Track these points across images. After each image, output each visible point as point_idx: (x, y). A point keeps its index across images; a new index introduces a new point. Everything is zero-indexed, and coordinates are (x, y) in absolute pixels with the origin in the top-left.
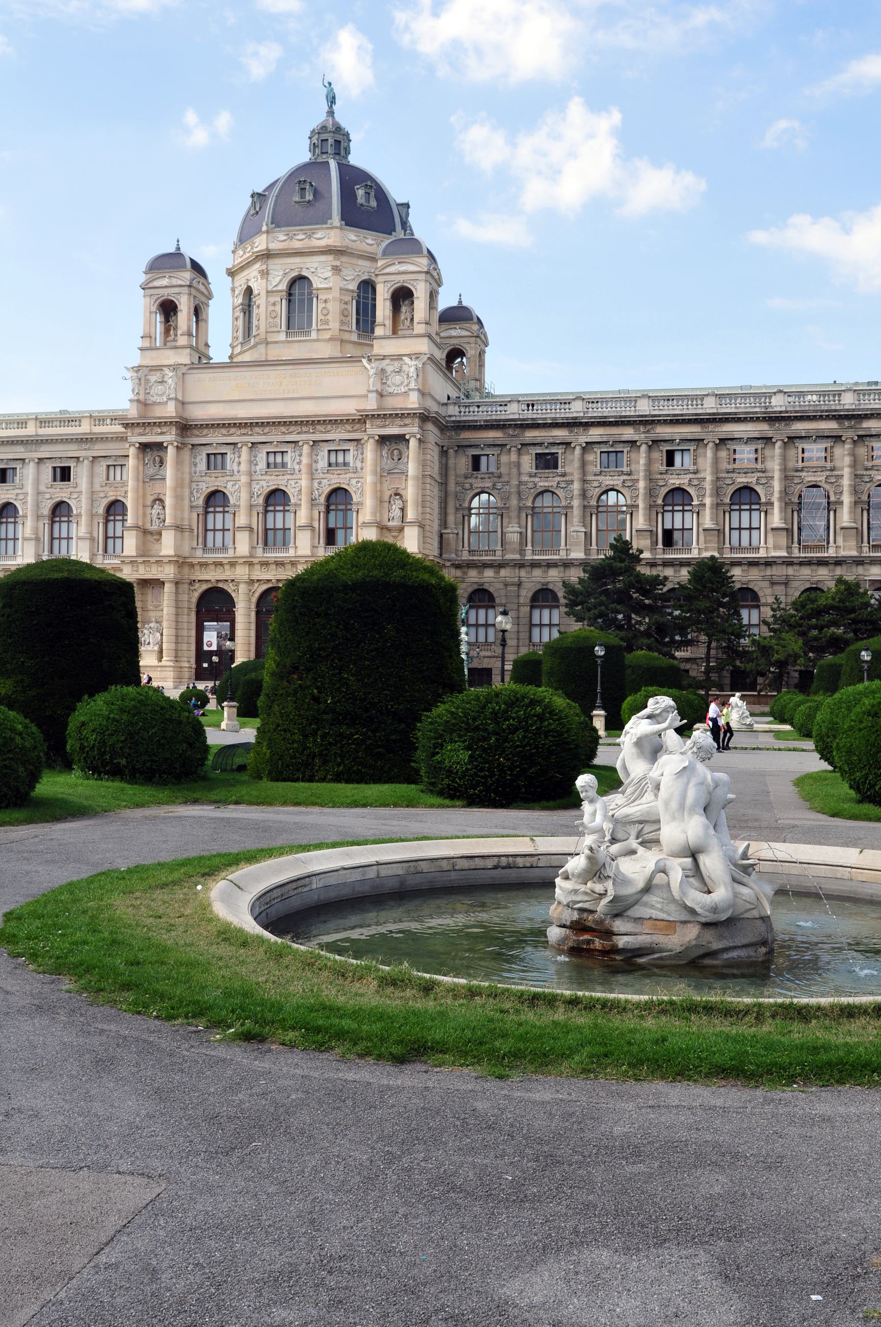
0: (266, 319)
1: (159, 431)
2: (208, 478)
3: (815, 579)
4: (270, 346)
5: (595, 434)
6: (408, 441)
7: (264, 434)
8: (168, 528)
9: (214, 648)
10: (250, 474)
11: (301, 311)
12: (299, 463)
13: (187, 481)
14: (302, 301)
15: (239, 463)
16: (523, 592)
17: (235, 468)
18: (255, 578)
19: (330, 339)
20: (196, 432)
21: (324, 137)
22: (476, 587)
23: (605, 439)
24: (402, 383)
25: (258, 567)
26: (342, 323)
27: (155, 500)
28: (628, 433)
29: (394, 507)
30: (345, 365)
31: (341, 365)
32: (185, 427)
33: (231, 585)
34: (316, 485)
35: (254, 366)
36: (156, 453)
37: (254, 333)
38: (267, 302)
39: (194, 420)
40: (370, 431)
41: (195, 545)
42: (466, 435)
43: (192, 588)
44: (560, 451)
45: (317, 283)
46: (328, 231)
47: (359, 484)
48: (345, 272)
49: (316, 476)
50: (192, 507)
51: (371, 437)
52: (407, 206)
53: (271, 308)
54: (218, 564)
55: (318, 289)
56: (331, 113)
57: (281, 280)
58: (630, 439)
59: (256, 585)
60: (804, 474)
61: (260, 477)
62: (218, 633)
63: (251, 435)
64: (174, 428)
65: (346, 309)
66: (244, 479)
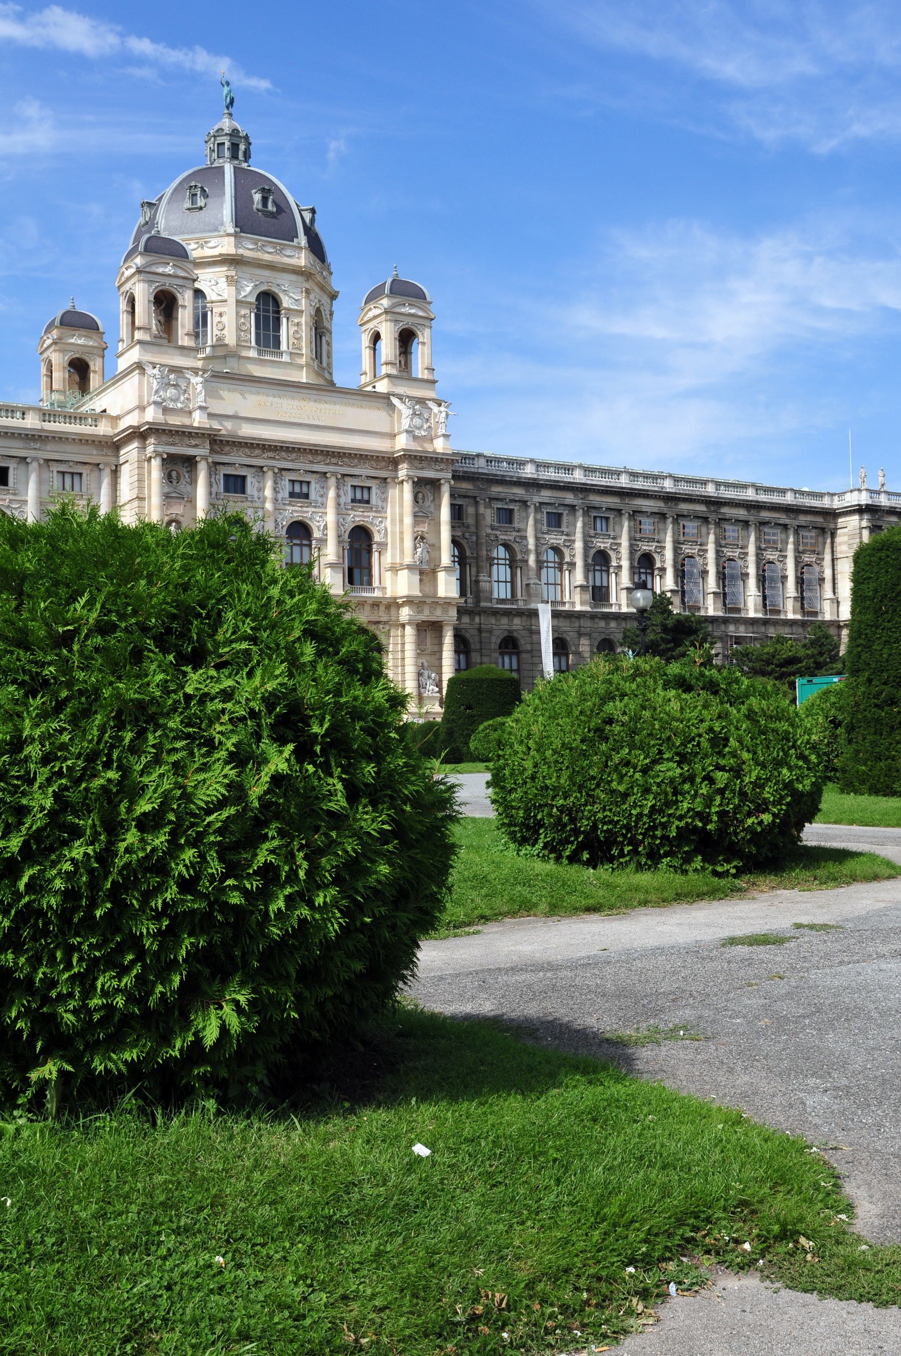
1: (194, 443)
4: (241, 361)
5: (546, 495)
7: (292, 461)
11: (266, 328)
16: (494, 640)
17: (256, 494)
21: (236, 141)
23: (552, 501)
28: (570, 498)
32: (216, 442)
35: (278, 384)
44: (516, 508)
45: (286, 302)
55: (289, 309)
58: (571, 503)
60: (684, 547)
63: (278, 460)
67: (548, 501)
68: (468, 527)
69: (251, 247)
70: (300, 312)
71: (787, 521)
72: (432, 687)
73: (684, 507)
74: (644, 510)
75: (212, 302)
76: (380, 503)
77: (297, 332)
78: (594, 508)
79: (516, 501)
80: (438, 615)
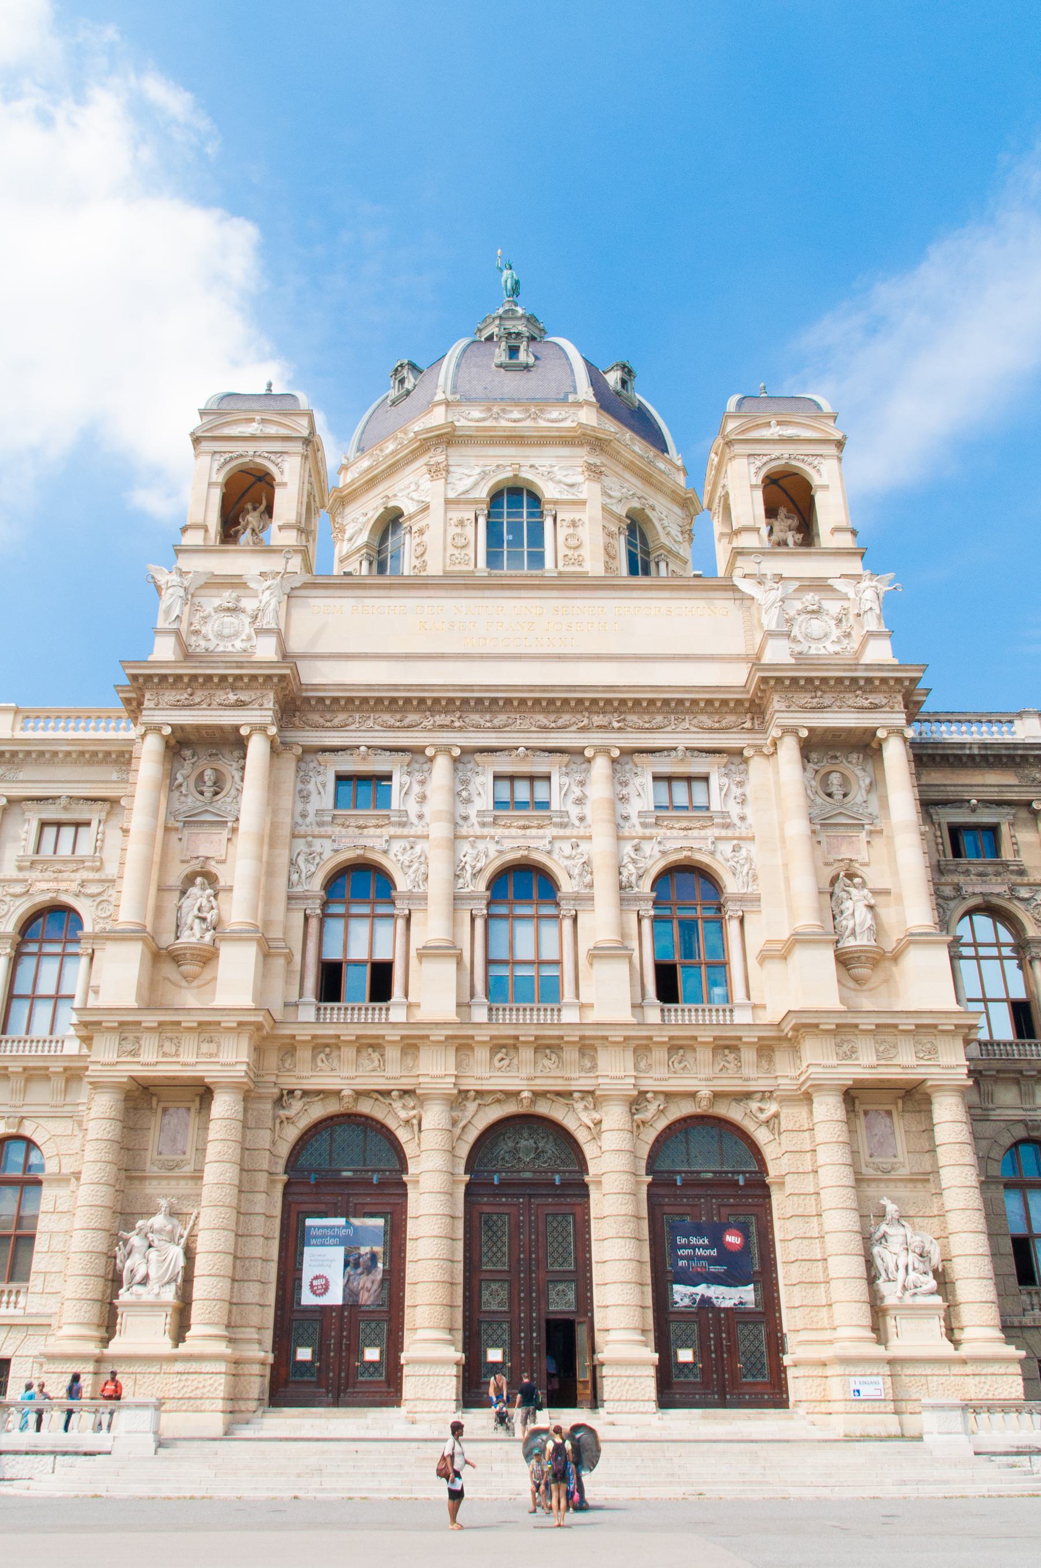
0: (445, 549)
2: (338, 830)
8: (237, 937)
9: (335, 1297)
10: (457, 821)
12: (580, 801)
13: (286, 831)
15: (423, 798)
17: (412, 808)
18: (470, 1084)
20: (316, 718)
25: (482, 1054)
27: (190, 880)
29: (848, 905)
30: (683, 594)
31: (675, 594)
33: (397, 1105)
34: (628, 848)
36: (203, 762)
38: (446, 521)
39: (315, 687)
41: (294, 997)
43: (283, 1113)
46: (572, 410)
47: (744, 852)
49: (626, 832)
50: (290, 898)
51: (792, 731)
53: (453, 530)
54: (371, 1045)
55: (556, 502)
57: (476, 484)
59: (471, 1107)
61: (478, 831)
62: (347, 1255)
63: (461, 729)
64: (271, 695)
65: (613, 547)
66: (439, 830)
72: (913, 1276)
75: (410, 518)
76: (734, 810)
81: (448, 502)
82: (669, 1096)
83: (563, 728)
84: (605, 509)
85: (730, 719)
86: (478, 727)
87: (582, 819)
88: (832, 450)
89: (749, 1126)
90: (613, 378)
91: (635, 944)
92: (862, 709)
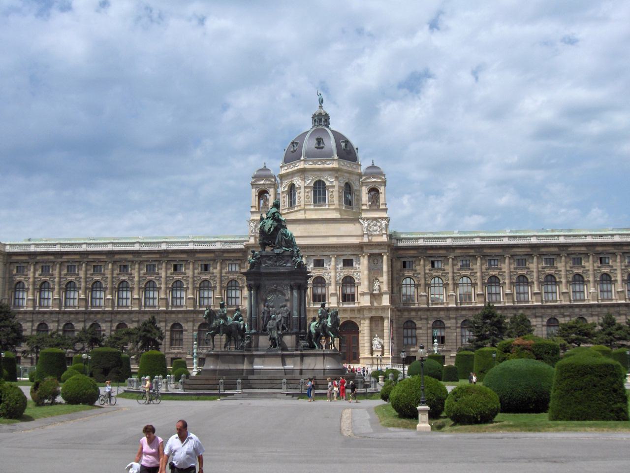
3: (553, 314)
6: (383, 256)
11: (320, 194)
12: (329, 265)
14: (320, 192)
19: (334, 209)
21: (320, 118)
22: (407, 320)
23: (462, 255)
24: (377, 230)
26: (339, 201)
28: (472, 252)
34: (338, 274)
37: (296, 205)
40: (365, 251)
42: (401, 252)
45: (328, 184)
48: (340, 178)
52: (357, 149)
53: (306, 194)
56: (321, 107)
57: (311, 182)
60: (545, 270)
67: (460, 255)
68: (416, 271)
69: (311, 163)
70: (333, 187)
71: (615, 251)
72: (378, 346)
73: (543, 250)
74: (518, 254)
77: (331, 195)
78: (488, 256)
79: (441, 257)
80: (380, 314)
81: (305, 187)
82: (343, 318)
83: (326, 251)
84: (340, 187)
85: (357, 249)
86: (311, 252)
87: (330, 268)
88: (383, 184)
89: (356, 322)
90: (343, 145)
91: (338, 293)
92: (380, 249)
